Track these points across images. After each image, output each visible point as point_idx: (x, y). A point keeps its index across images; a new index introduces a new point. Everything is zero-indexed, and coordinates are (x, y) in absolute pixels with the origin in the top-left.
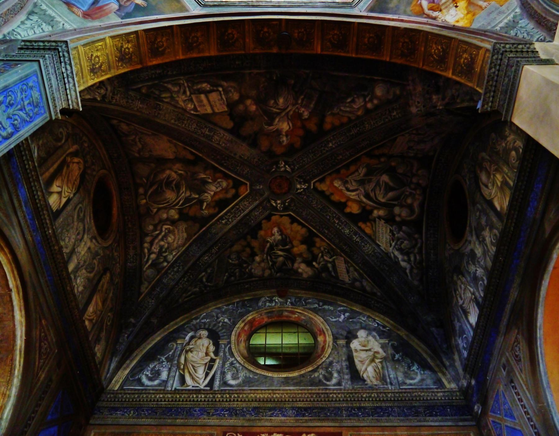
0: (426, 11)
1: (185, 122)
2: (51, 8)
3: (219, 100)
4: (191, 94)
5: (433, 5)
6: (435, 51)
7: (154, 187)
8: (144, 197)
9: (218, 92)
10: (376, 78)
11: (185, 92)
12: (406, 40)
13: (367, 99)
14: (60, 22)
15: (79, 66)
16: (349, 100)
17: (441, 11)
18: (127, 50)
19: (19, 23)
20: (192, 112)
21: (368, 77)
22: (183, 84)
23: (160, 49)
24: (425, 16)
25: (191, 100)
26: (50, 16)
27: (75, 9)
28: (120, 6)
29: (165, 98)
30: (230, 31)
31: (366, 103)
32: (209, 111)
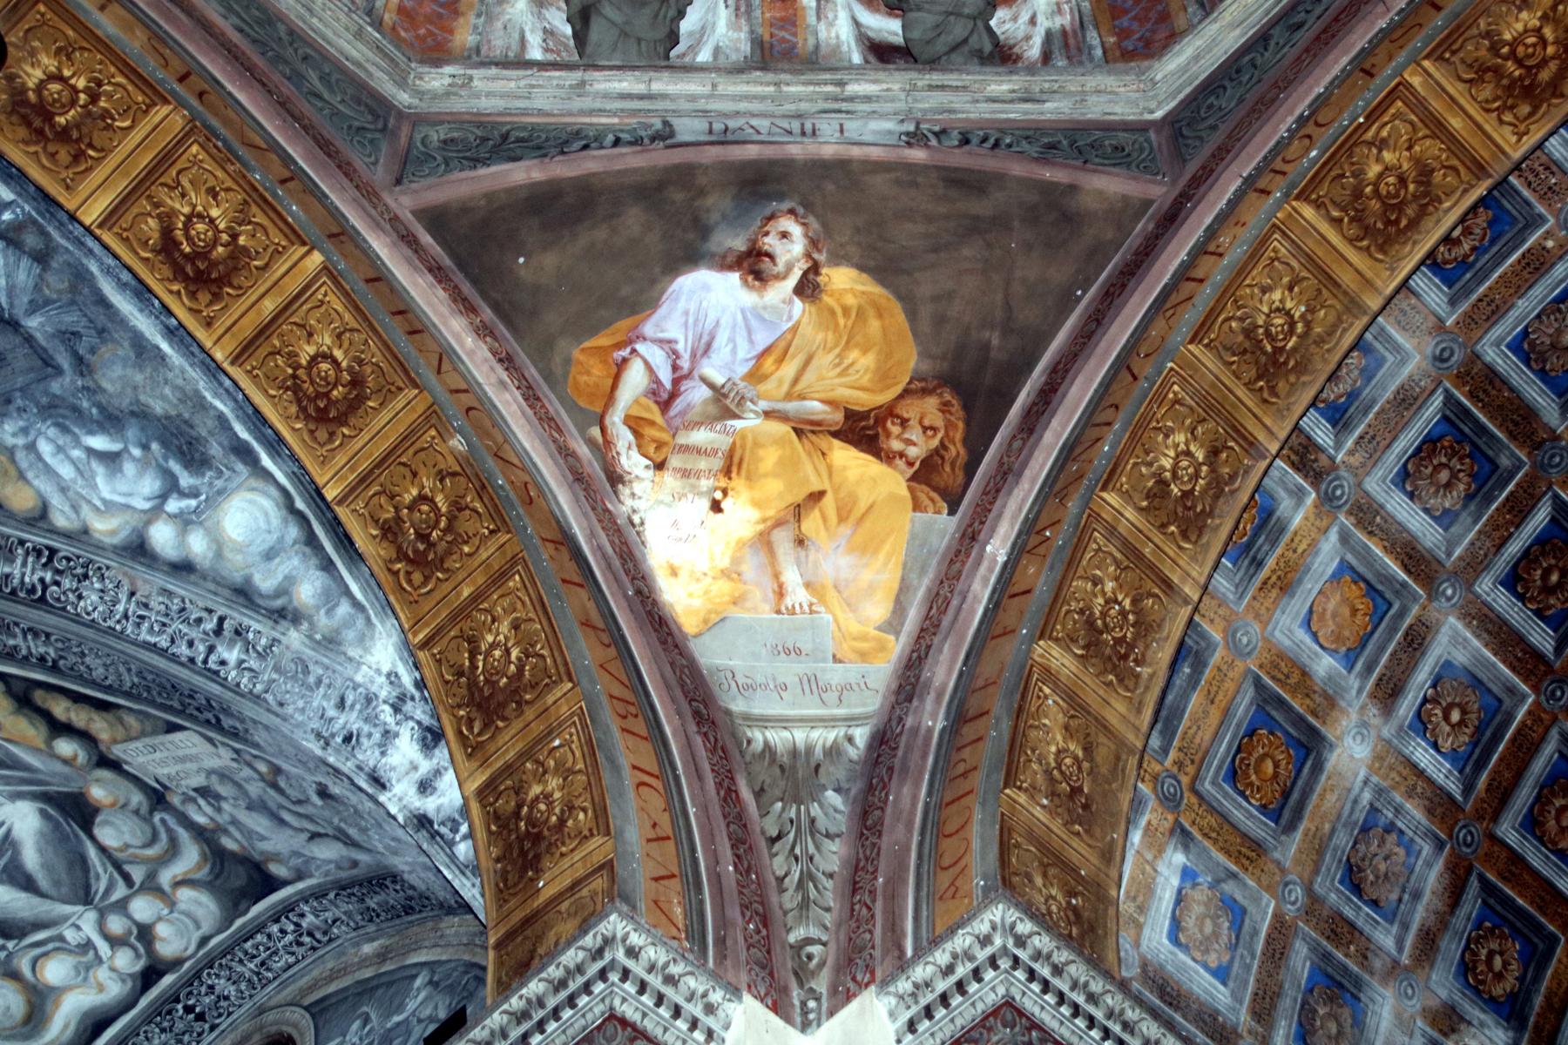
0: (616, 419)
5: (656, 416)
6: (494, 646)
10: (266, 461)
12: (439, 499)
13: (173, 505)
16: (99, 442)
17: (660, 466)
21: (244, 434)
24: (595, 432)
31: (157, 511)
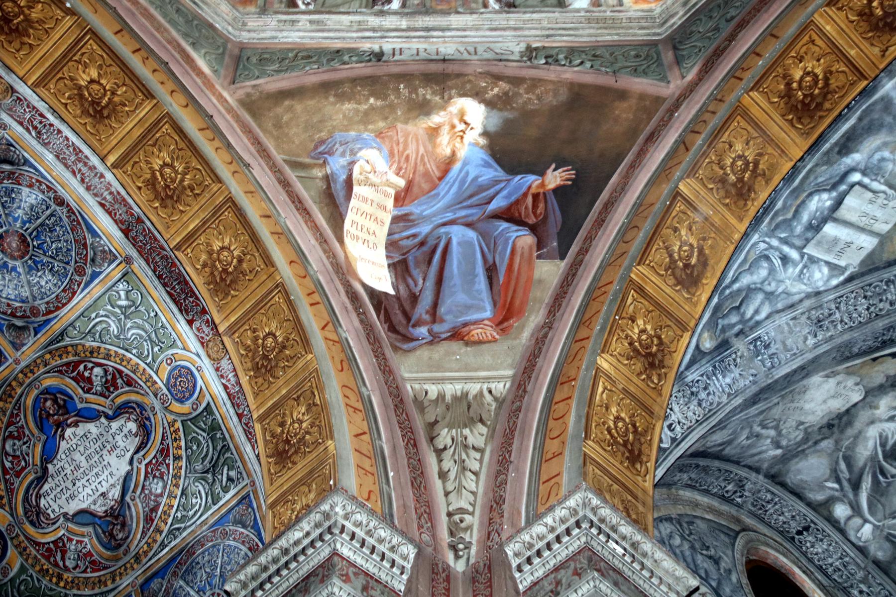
1: (838, 315)
2: (442, 380)
3: (871, 202)
4: (800, 249)
7: (867, 484)
8: (857, 521)
9: (857, 187)
11: (785, 259)
14: (481, 393)
15: (615, 487)
18: (644, 337)
19: (438, 483)
20: (835, 282)
22: (771, 247)
23: (694, 261)
25: (813, 260)
26: (455, 398)
27: (477, 333)
28: (533, 229)
29: (757, 312)
30: (797, 74)
32: (868, 243)
